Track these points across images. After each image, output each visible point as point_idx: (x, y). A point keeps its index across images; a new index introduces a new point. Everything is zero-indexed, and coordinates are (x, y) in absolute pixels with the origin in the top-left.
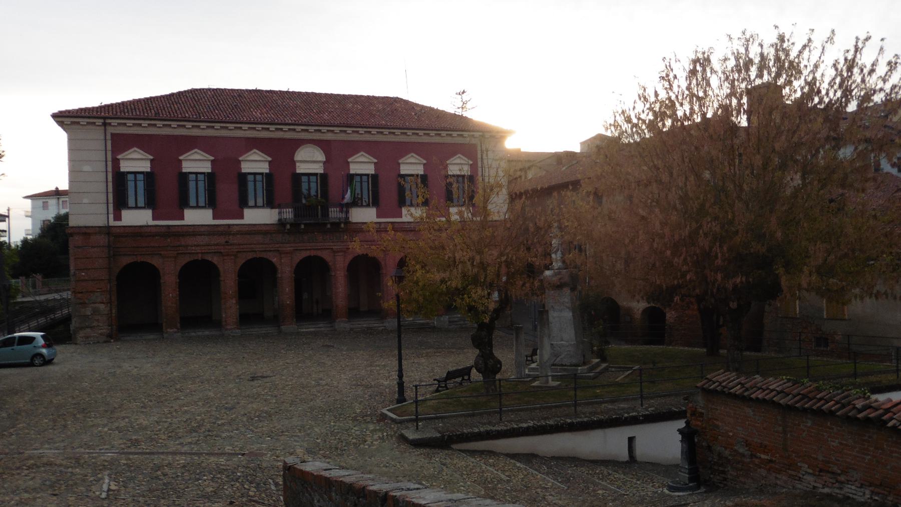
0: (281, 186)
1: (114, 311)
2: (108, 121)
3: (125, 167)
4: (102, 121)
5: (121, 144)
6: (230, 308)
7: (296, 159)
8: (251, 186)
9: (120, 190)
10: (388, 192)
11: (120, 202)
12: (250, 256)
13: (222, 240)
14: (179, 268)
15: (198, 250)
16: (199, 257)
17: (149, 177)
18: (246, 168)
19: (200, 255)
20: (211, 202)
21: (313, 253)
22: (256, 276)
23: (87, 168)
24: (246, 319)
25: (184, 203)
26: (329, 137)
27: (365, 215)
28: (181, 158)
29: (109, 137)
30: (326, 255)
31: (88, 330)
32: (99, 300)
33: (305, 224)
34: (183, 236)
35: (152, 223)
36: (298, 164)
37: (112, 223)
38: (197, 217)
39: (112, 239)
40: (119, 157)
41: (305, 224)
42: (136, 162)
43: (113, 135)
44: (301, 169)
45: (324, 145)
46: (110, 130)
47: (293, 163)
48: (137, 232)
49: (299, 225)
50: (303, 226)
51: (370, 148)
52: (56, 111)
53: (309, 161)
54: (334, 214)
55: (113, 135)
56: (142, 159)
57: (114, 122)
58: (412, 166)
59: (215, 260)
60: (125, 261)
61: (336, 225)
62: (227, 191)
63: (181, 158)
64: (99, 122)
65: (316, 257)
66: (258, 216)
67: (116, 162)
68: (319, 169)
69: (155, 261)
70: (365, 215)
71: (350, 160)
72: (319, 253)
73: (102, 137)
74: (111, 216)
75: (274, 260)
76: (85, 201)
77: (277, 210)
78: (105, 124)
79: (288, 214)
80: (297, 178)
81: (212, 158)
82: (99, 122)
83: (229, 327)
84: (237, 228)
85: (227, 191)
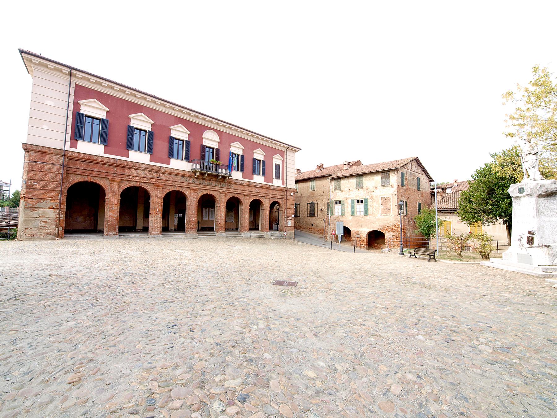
0: (192, 150)
1: (62, 216)
2: (73, 71)
3: (84, 110)
4: (69, 70)
5: (82, 93)
6: (155, 220)
7: (203, 136)
8: (175, 146)
9: (78, 126)
10: (248, 165)
11: (77, 134)
12: (172, 189)
13: (154, 175)
14: (121, 190)
15: (138, 179)
16: (138, 185)
17: (104, 123)
18: (174, 134)
19: (138, 183)
20: (150, 150)
21: (209, 192)
22: (175, 201)
23: (48, 102)
24: (165, 229)
25: (130, 145)
26: (222, 129)
27: (237, 175)
28: (130, 116)
29: (73, 85)
30: (215, 194)
31: (35, 229)
32: (49, 206)
33: (208, 174)
34: (127, 168)
35: (102, 154)
36: (204, 140)
37: (68, 148)
38: (139, 157)
39: (66, 160)
40: (80, 102)
41: (208, 174)
42: (94, 109)
43: (76, 85)
44: (206, 143)
45: (219, 133)
46: (75, 81)
47: (202, 138)
48: (90, 160)
49: (205, 173)
50: (207, 175)
51: (242, 140)
52: (25, 49)
53: (211, 139)
54: (223, 172)
55: (76, 85)
56: (101, 109)
57: (80, 75)
58: (259, 155)
59: (148, 188)
60: (77, 179)
61: (224, 177)
62: (161, 146)
63: (130, 116)
64: (67, 70)
65: (210, 195)
66: (179, 164)
67: (77, 105)
68: (215, 146)
69: (102, 182)
70: (237, 175)
71: (231, 144)
72: (212, 193)
73: (68, 84)
74: (68, 144)
75: (187, 193)
76: (45, 127)
77: (190, 164)
78: (71, 74)
79: (198, 166)
80: (203, 148)
81: (153, 122)
82: (67, 70)
83: (154, 233)
84: (166, 169)
85: (161, 146)
